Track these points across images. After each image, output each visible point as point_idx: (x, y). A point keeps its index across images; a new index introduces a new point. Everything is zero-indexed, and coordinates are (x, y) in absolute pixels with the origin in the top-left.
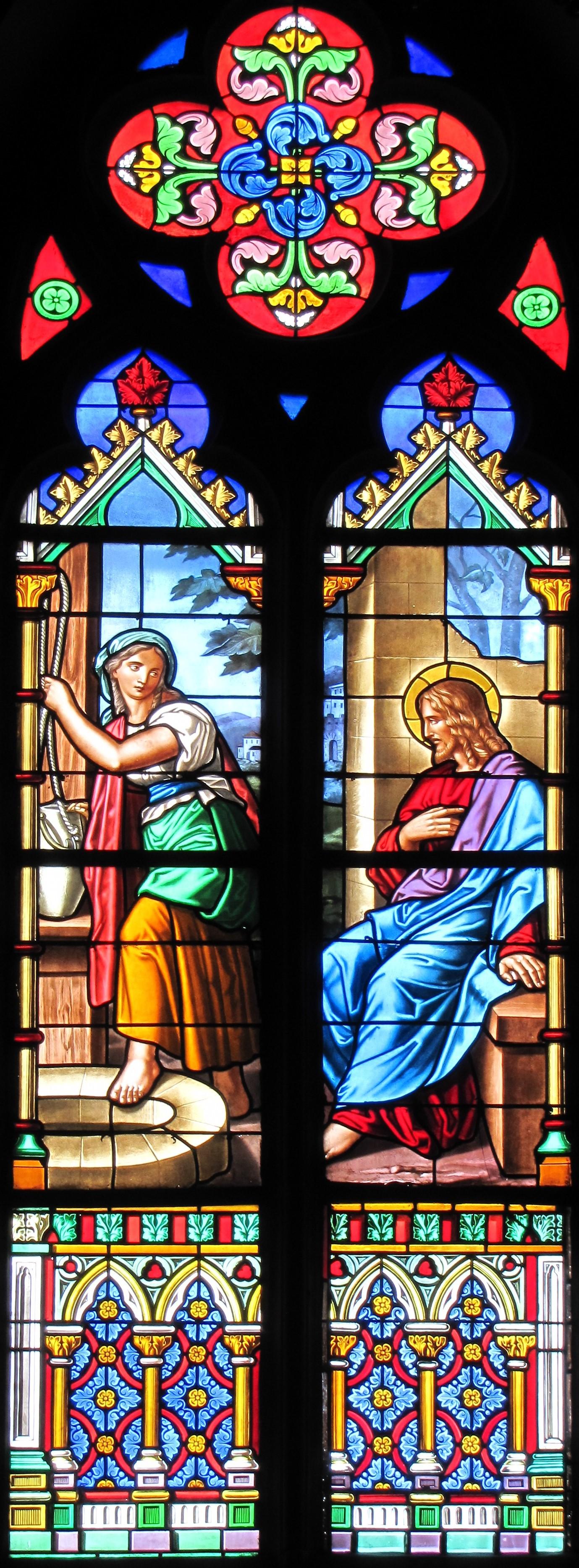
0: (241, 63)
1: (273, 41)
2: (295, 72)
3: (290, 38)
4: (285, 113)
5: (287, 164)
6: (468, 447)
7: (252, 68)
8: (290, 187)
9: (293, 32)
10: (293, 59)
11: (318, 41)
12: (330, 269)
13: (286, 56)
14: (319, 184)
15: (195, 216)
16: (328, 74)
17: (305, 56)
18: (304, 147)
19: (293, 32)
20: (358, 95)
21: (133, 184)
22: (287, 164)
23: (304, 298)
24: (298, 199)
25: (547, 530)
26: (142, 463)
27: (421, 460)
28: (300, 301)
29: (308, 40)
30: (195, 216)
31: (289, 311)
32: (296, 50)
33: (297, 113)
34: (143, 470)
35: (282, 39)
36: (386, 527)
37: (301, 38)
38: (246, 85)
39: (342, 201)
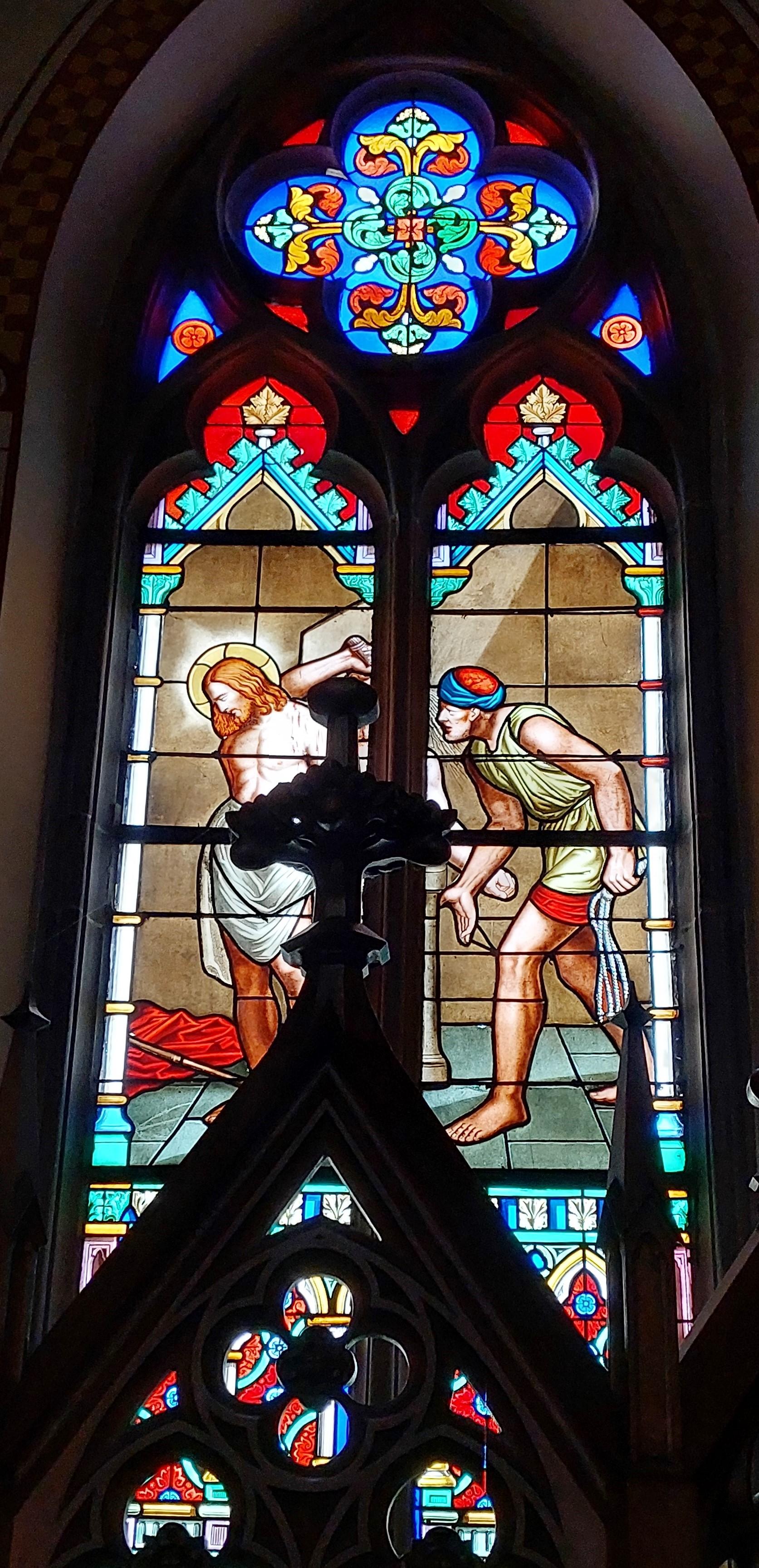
0: (366, 148)
1: (393, 128)
2: (413, 152)
3: (408, 125)
4: (402, 183)
5: (404, 223)
6: (563, 456)
7: (374, 151)
8: (404, 242)
9: (410, 120)
10: (409, 141)
11: (433, 127)
12: (437, 308)
13: (404, 140)
14: (430, 238)
15: (321, 265)
16: (440, 153)
17: (420, 140)
18: (417, 210)
19: (410, 120)
20: (467, 168)
21: (268, 240)
22: (404, 223)
23: (414, 332)
24: (411, 251)
25: (641, 529)
26: (263, 474)
27: (518, 471)
28: (411, 335)
29: (424, 126)
30: (321, 265)
31: (399, 343)
32: (412, 136)
33: (412, 183)
34: (262, 482)
35: (400, 126)
36: (488, 528)
37: (417, 125)
38: (370, 163)
39: (450, 252)
